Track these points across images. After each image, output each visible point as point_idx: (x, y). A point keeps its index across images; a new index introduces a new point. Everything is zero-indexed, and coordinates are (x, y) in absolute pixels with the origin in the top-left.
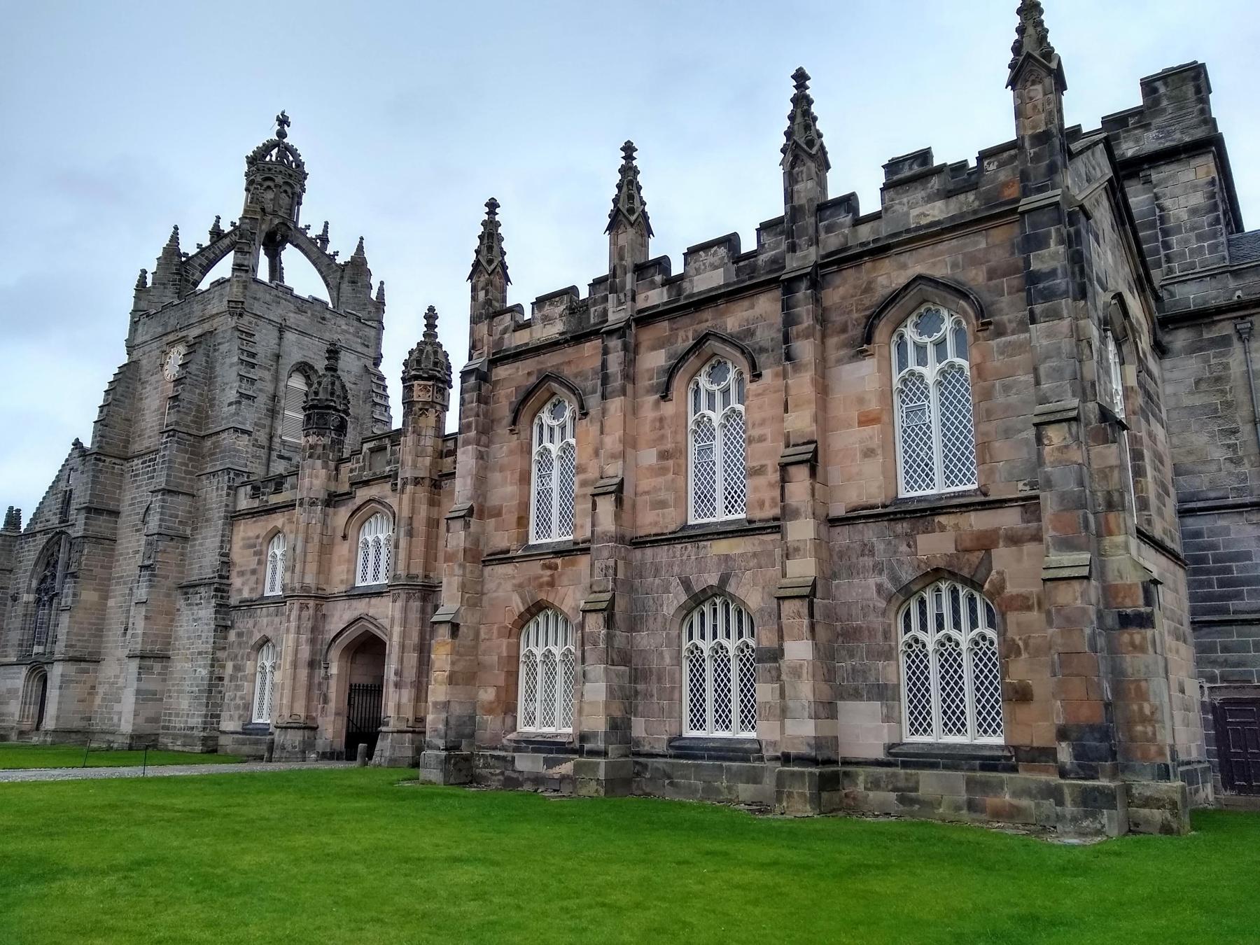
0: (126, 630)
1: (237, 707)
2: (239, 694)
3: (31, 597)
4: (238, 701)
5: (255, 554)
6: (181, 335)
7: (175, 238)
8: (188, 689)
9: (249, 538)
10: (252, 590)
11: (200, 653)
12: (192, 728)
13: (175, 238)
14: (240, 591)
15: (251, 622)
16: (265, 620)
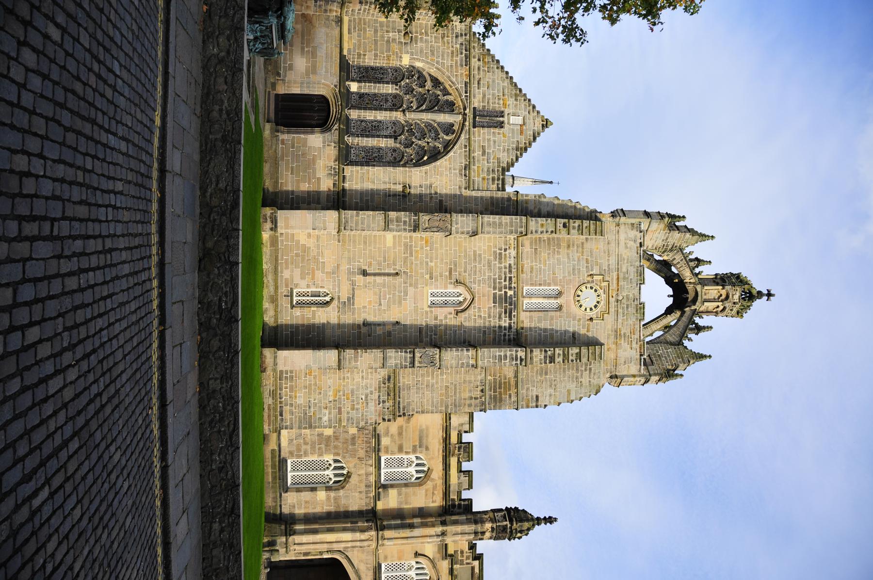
0: (365, 273)
1: (299, 450)
2: (308, 447)
3: (406, 61)
4: (304, 447)
5: (415, 447)
6: (612, 310)
7: (703, 237)
8: (312, 400)
9: (427, 436)
10: (387, 448)
11: (340, 412)
12: (281, 415)
13: (703, 237)
14: (387, 434)
15: (362, 453)
16: (363, 472)
